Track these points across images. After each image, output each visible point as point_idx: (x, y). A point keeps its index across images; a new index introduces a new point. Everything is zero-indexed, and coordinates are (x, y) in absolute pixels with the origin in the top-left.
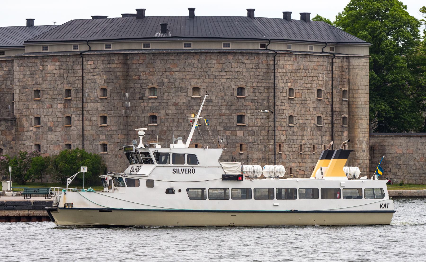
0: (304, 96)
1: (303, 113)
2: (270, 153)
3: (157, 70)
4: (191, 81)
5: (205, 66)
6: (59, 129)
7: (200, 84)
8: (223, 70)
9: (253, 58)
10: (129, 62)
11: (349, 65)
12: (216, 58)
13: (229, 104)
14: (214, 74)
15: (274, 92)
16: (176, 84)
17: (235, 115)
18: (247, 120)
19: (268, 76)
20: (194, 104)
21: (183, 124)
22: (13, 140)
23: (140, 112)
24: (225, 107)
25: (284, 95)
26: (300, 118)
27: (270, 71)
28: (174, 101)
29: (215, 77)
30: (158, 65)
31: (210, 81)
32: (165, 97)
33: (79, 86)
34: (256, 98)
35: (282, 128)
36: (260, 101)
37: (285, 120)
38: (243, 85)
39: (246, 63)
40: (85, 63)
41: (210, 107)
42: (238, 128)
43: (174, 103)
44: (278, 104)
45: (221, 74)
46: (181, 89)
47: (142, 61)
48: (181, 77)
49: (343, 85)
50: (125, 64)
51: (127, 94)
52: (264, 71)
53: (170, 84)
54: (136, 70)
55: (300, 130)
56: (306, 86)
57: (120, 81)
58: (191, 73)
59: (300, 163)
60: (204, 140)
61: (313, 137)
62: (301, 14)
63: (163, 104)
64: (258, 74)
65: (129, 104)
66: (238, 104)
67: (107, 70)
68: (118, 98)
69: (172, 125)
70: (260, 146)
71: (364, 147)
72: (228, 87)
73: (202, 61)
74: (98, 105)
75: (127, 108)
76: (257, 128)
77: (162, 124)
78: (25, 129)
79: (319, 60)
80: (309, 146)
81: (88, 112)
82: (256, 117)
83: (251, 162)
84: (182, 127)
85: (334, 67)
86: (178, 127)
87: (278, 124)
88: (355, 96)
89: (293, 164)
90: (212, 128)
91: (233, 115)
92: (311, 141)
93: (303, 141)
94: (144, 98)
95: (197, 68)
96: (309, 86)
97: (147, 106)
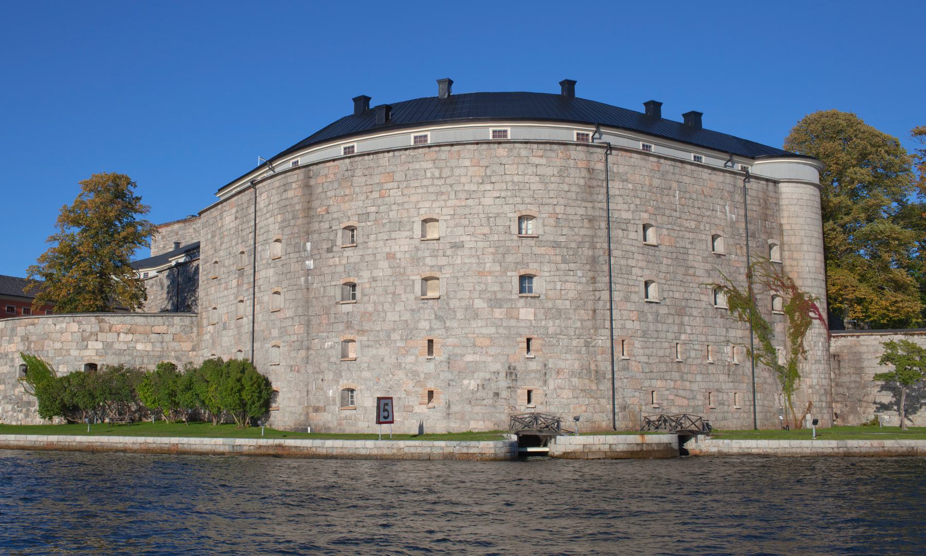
0: (681, 243)
1: (680, 277)
2: (599, 358)
3: (357, 189)
4: (421, 205)
5: (449, 174)
7: (438, 211)
9: (553, 155)
10: (312, 182)
11: (778, 199)
12: (471, 156)
13: (501, 250)
14: (466, 188)
15: (608, 228)
16: (391, 214)
17: (513, 273)
18: (537, 285)
19: (591, 194)
20: (427, 253)
21: (403, 297)
22: (193, 350)
23: (328, 278)
24: (491, 257)
25: (632, 235)
26: (674, 288)
27: (595, 183)
28: (388, 250)
29: (470, 195)
30: (359, 180)
31: (457, 203)
32: (370, 244)
34: (563, 239)
35: (629, 306)
36: (573, 245)
37: (637, 289)
38: (532, 210)
39: (537, 166)
41: (459, 258)
42: (522, 301)
43: (387, 254)
44: (615, 253)
45: (482, 188)
46: (400, 225)
47: (332, 176)
48: (400, 200)
49: (770, 235)
51: (309, 245)
52: (582, 182)
53: (379, 216)
54: (323, 196)
55: (673, 312)
56: (686, 224)
57: (299, 222)
58: (420, 191)
59: (675, 381)
60: (447, 329)
61: (705, 330)
62: (684, 115)
63: (367, 258)
64: (566, 188)
65: (310, 264)
66: (521, 251)
67: (282, 203)
68: (297, 255)
69: (382, 299)
70: (575, 343)
71: (819, 353)
72: (498, 215)
73: (442, 164)
75: (308, 272)
76: (568, 302)
77: (366, 298)
79: (713, 177)
80: (696, 347)
82: (563, 279)
83: (554, 376)
84: (402, 304)
85: (748, 198)
86: (394, 303)
87: (617, 296)
88: (795, 255)
89: (659, 384)
90: (463, 304)
91: (509, 274)
92: (703, 338)
93: (683, 337)
94: (335, 249)
95: (433, 178)
96: (693, 225)
97: (340, 264)
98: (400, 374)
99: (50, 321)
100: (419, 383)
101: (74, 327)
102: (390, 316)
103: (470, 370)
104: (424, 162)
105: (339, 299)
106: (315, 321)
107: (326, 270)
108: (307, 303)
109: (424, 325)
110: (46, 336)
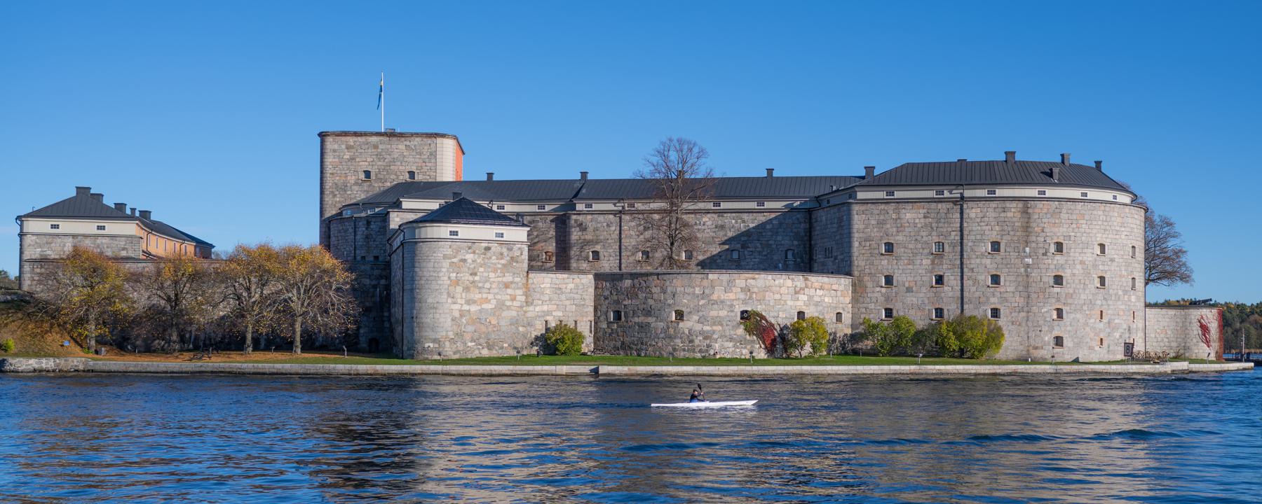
6: (924, 290)
8: (1122, 225)
30: (1064, 216)
33: (958, 238)
40: (966, 211)
46: (1087, 245)
50: (1025, 212)
51: (1027, 250)
65: (1029, 261)
74: (988, 261)
75: (1028, 266)
78: (868, 290)
81: (972, 270)
98: (1088, 329)
99: (770, 277)
100: (1096, 334)
101: (789, 283)
102: (1083, 297)
103: (1115, 328)
104: (1099, 211)
105: (1052, 283)
106: (1034, 296)
107: (1042, 266)
108: (1027, 286)
109: (1099, 302)
110: (767, 289)
